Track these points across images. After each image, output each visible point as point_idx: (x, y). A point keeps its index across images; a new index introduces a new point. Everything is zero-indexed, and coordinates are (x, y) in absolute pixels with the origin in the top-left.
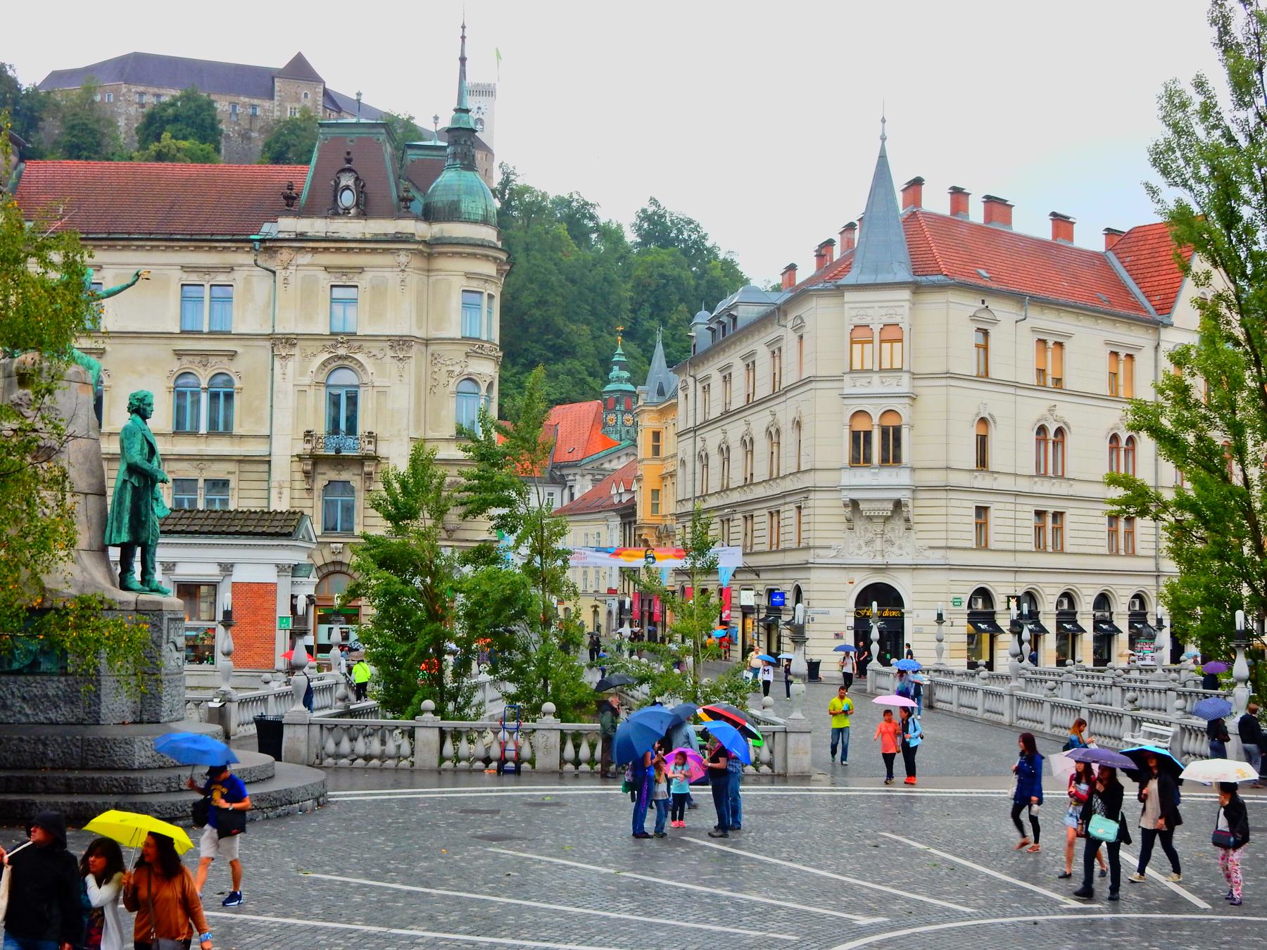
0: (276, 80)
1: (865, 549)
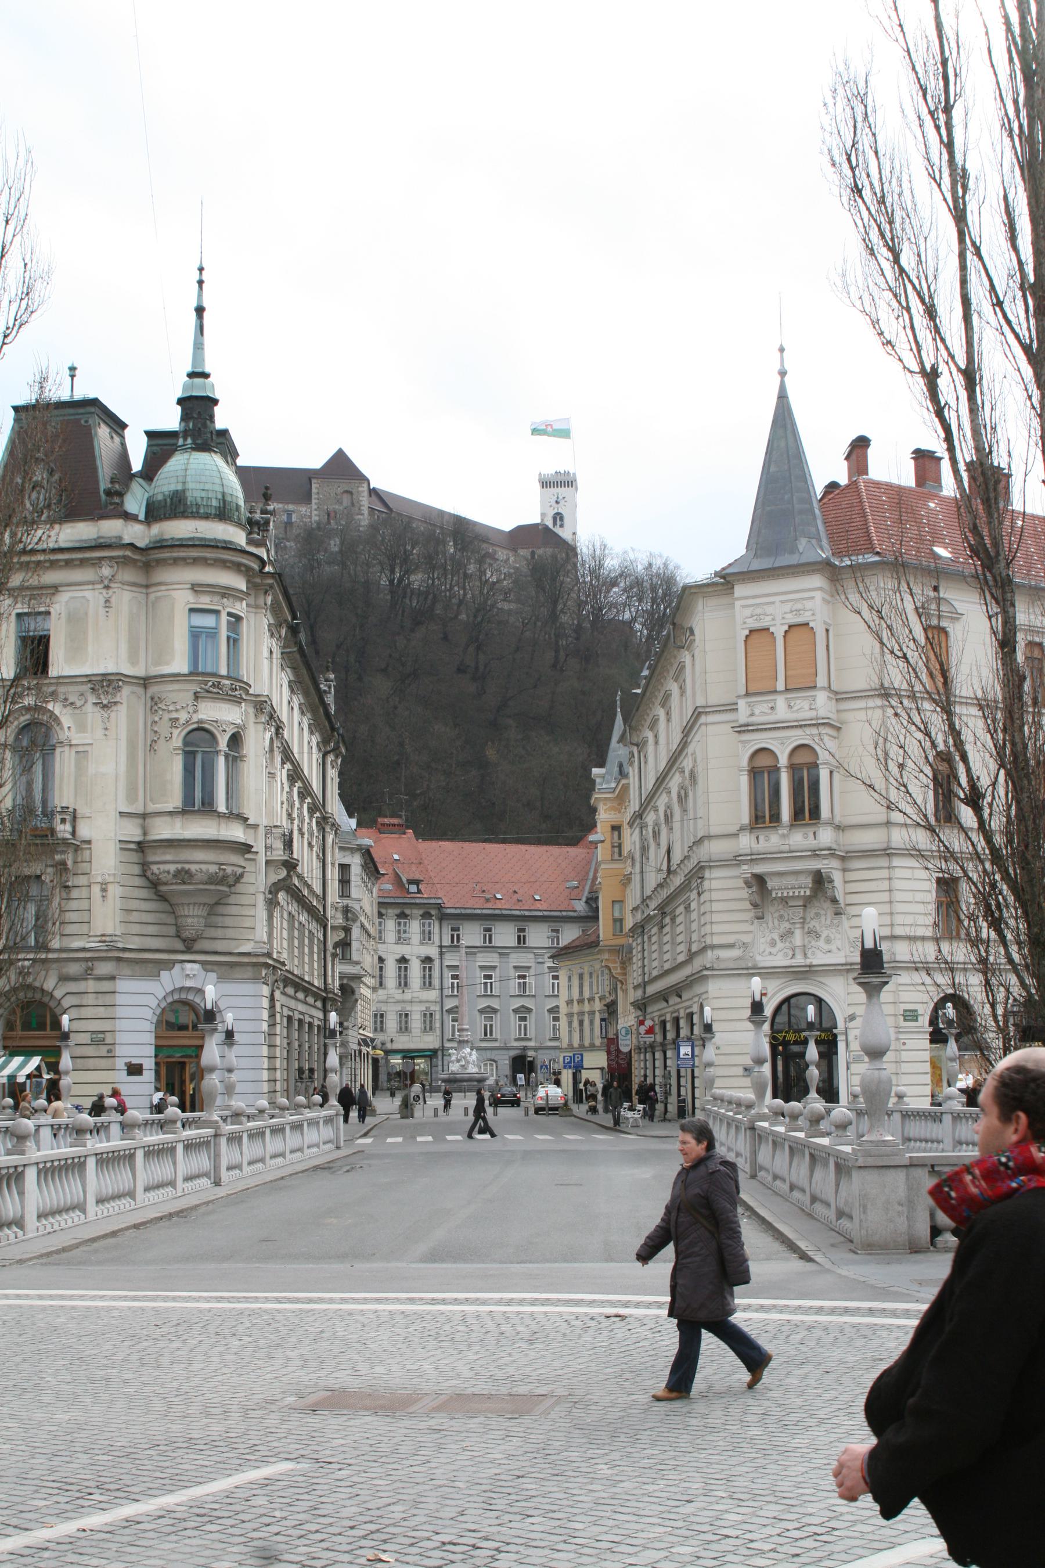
0: (313, 481)
1: (780, 945)
